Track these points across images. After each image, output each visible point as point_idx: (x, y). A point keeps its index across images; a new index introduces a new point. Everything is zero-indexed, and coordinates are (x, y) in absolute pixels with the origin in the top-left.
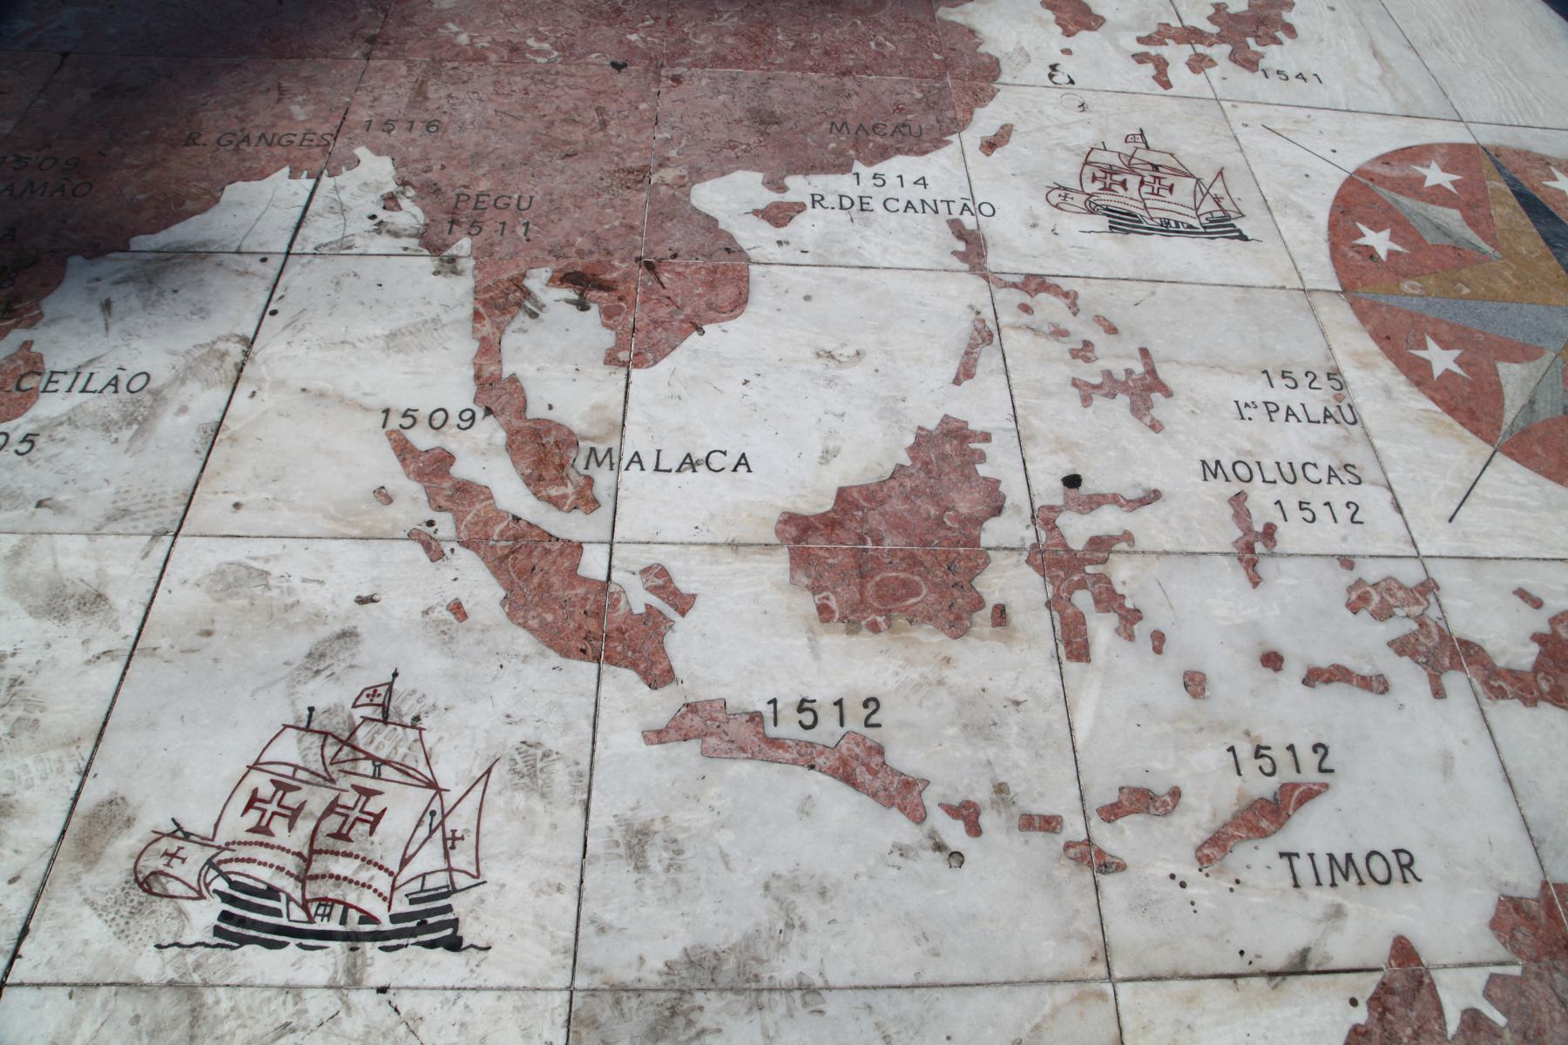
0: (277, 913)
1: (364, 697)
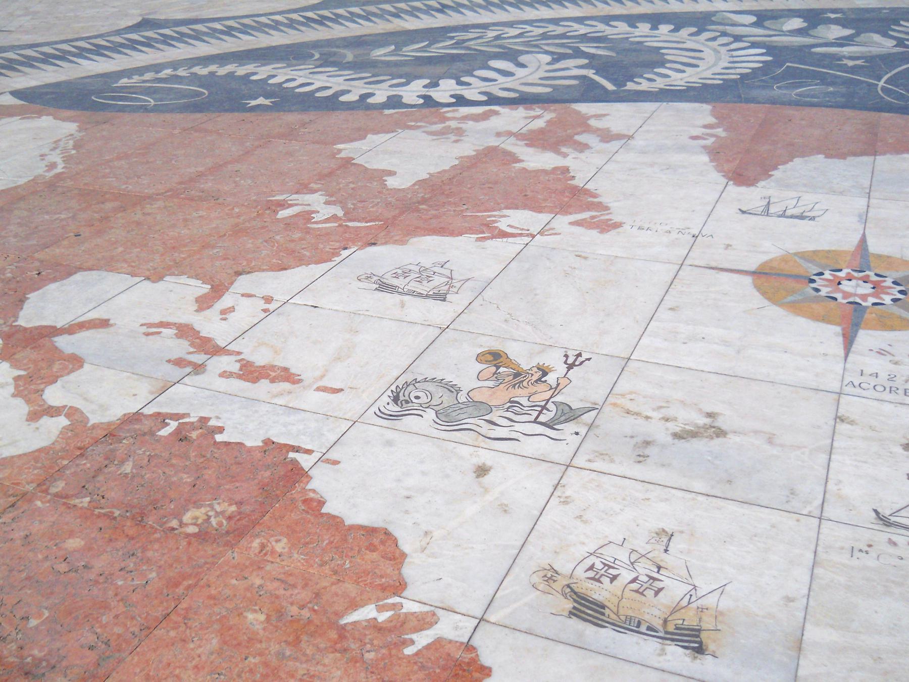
0: (603, 614)
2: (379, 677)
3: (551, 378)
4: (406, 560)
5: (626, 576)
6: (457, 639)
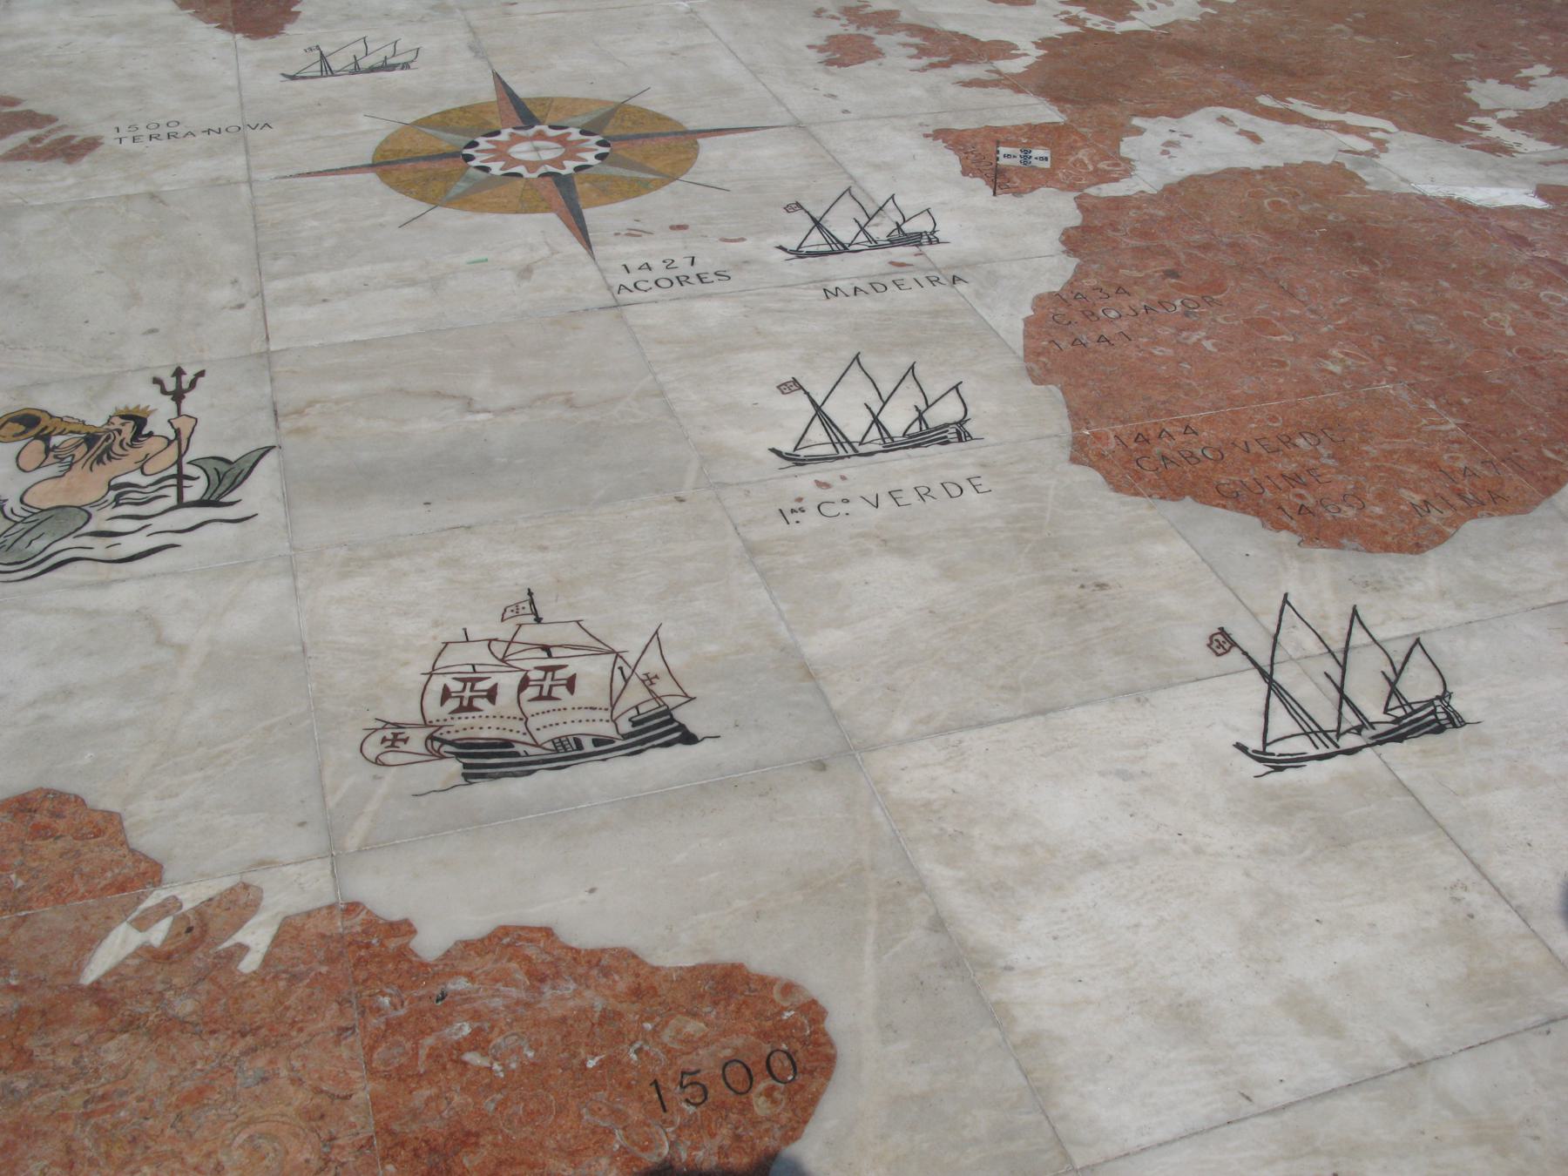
2: (230, 1032)
3: (158, 424)
4: (126, 824)
5: (508, 682)
6: (319, 904)
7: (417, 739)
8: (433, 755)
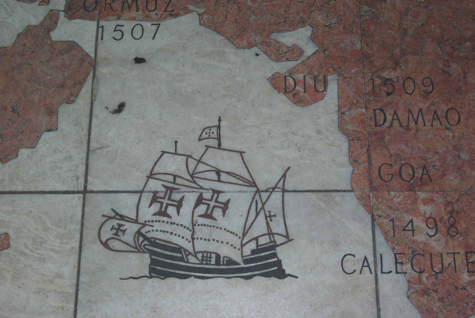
0: (182, 259)
1: (204, 134)
7: (131, 228)
8: (136, 248)
